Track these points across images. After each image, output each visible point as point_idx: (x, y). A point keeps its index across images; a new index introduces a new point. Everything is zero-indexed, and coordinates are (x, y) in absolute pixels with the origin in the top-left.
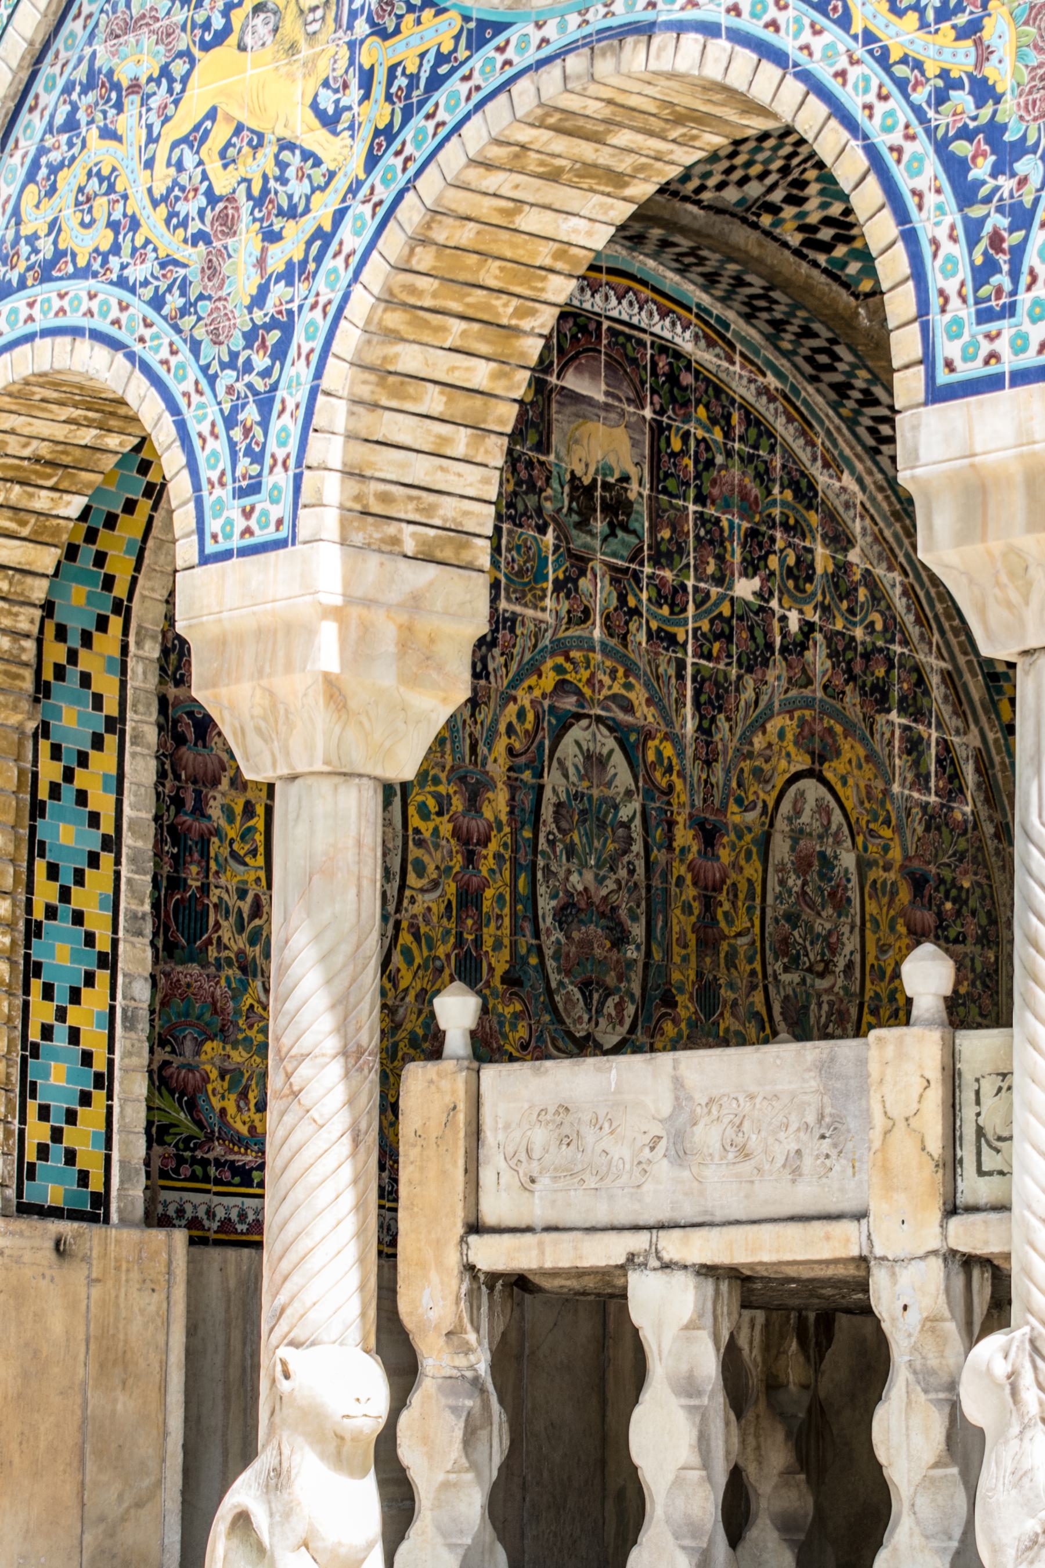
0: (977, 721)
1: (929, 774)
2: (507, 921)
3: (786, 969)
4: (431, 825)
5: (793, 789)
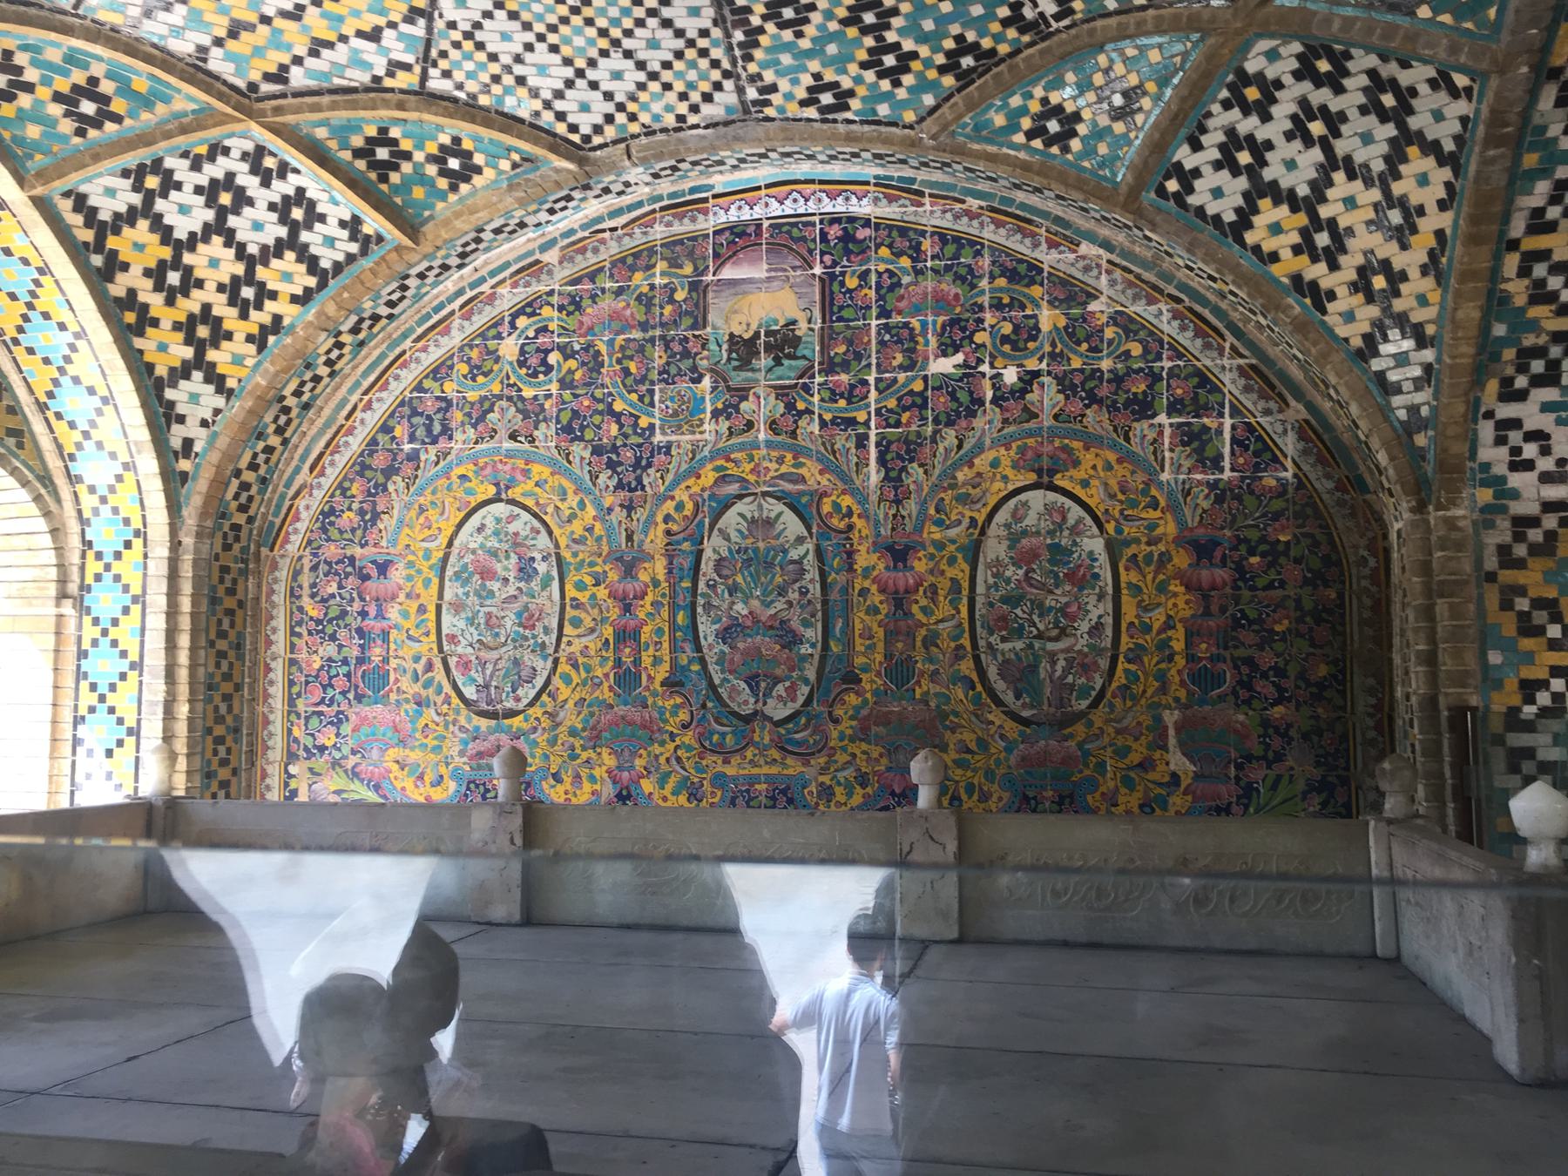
1: (1220, 457)
2: (666, 645)
3: (1004, 639)
4: (587, 594)
5: (1012, 503)
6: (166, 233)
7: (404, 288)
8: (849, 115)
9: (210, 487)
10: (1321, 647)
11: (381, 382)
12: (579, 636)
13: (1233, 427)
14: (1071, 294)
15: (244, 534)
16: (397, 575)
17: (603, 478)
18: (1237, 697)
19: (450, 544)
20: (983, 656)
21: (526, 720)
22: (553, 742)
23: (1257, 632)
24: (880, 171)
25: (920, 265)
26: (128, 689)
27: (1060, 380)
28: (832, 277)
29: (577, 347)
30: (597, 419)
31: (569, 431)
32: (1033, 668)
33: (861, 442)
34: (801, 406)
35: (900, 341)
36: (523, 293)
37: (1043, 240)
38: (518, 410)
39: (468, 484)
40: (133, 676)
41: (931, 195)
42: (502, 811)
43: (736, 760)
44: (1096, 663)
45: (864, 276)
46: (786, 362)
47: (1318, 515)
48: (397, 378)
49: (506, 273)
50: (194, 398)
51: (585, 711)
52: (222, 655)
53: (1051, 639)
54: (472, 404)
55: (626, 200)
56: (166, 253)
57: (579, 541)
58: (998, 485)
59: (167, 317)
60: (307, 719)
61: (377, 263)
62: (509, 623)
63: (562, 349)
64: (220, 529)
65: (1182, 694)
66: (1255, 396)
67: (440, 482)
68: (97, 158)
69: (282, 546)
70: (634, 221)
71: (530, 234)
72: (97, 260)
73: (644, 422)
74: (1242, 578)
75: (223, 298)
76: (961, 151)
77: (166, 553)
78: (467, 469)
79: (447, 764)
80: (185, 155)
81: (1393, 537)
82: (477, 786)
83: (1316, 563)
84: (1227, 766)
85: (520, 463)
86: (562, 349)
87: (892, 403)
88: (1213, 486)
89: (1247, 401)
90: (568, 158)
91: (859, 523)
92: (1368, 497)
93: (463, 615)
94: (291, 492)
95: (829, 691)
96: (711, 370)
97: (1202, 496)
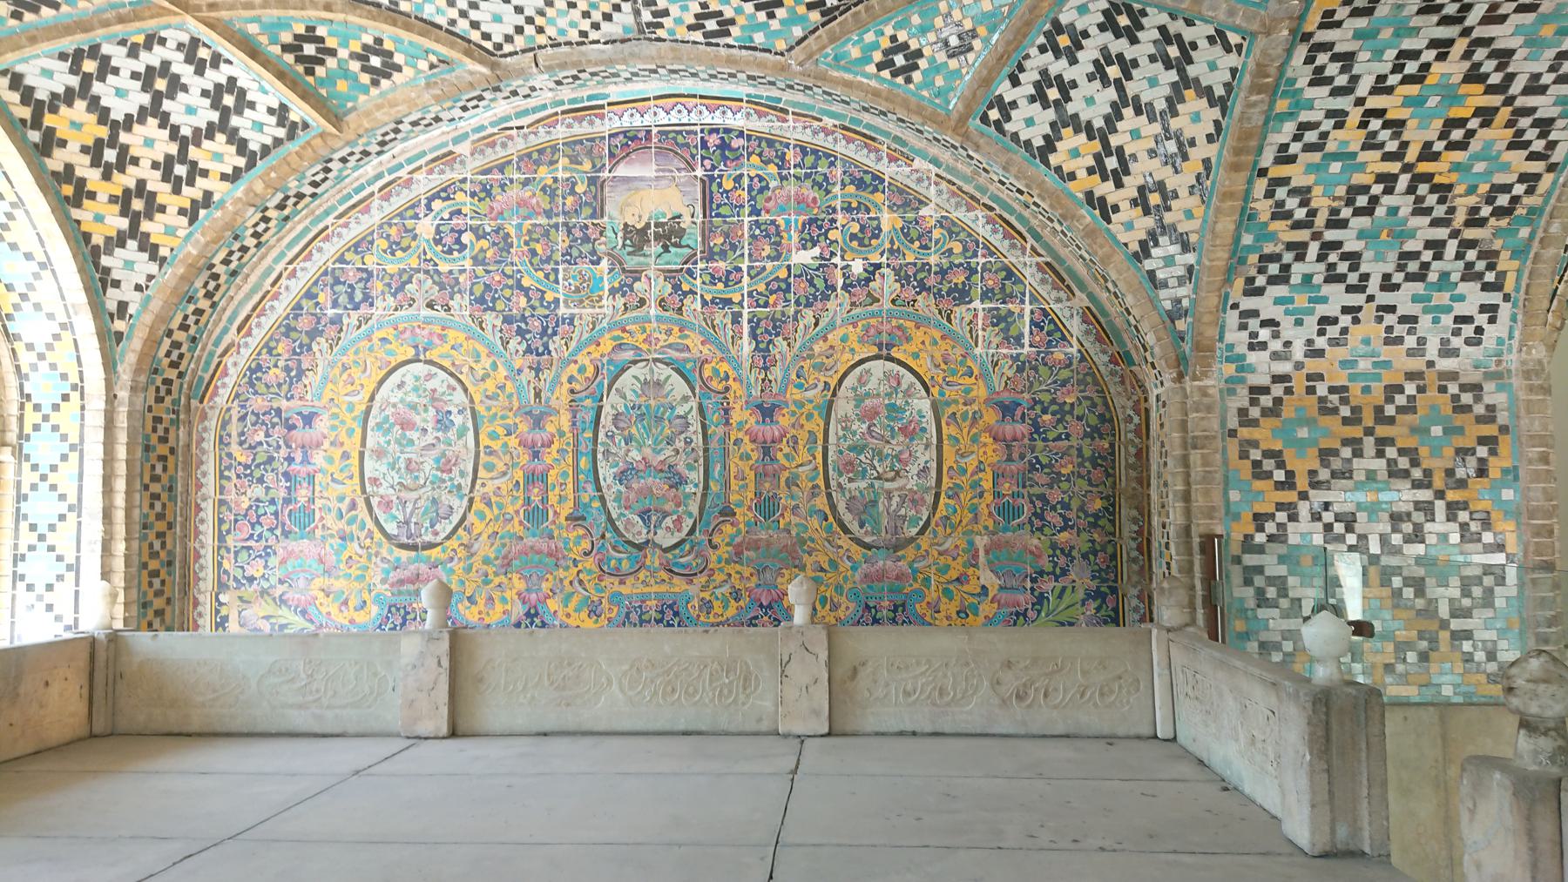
1: (1020, 336)
2: (570, 486)
3: (851, 480)
4: (500, 443)
5: (858, 370)
6: (103, 115)
7: (328, 170)
8: (729, 40)
9: (144, 345)
10: (1097, 486)
11: (305, 253)
12: (492, 479)
13: (1032, 312)
14: (908, 201)
15: (175, 388)
16: (322, 425)
17: (513, 344)
18: (1032, 526)
19: (372, 399)
20: (834, 494)
21: (444, 551)
22: (468, 570)
23: (1048, 474)
24: (752, 91)
25: (785, 172)
26: (67, 529)
27: (897, 272)
28: (712, 178)
29: (488, 229)
30: (507, 293)
31: (483, 301)
32: (874, 503)
33: (736, 318)
34: (685, 287)
35: (768, 236)
36: (437, 180)
37: (884, 155)
38: (434, 282)
39: (388, 346)
40: (72, 517)
41: (793, 113)
42: (430, 638)
43: (630, 580)
44: (922, 499)
45: (738, 179)
46: (672, 249)
47: (1096, 383)
48: (320, 250)
49: (422, 161)
50: (129, 265)
51: (498, 542)
52: (156, 497)
53: (887, 480)
54: (392, 276)
55: (531, 102)
56: (104, 132)
58: (847, 356)
59: (104, 190)
60: (236, 553)
61: (303, 148)
62: (427, 467)
63: (474, 230)
64: (153, 383)
65: (990, 523)
66: (1049, 287)
67: (363, 344)
68: (33, 40)
69: (211, 399)
70: (538, 121)
71: (444, 127)
72: (35, 136)
73: (549, 297)
74: (1037, 432)
75: (158, 174)
76: (823, 77)
77: (102, 405)
78: (388, 332)
79: (370, 591)
80: (123, 42)
81: (1152, 400)
82: (398, 610)
83: (1093, 420)
84: (1024, 580)
85: (437, 329)
86: (474, 230)
87: (762, 288)
88: (1016, 358)
89: (1044, 291)
90: (481, 62)
91: (734, 386)
92: (1133, 368)
93: (385, 461)
94: (220, 350)
95: (709, 523)
96: (609, 254)
97: (1007, 366)
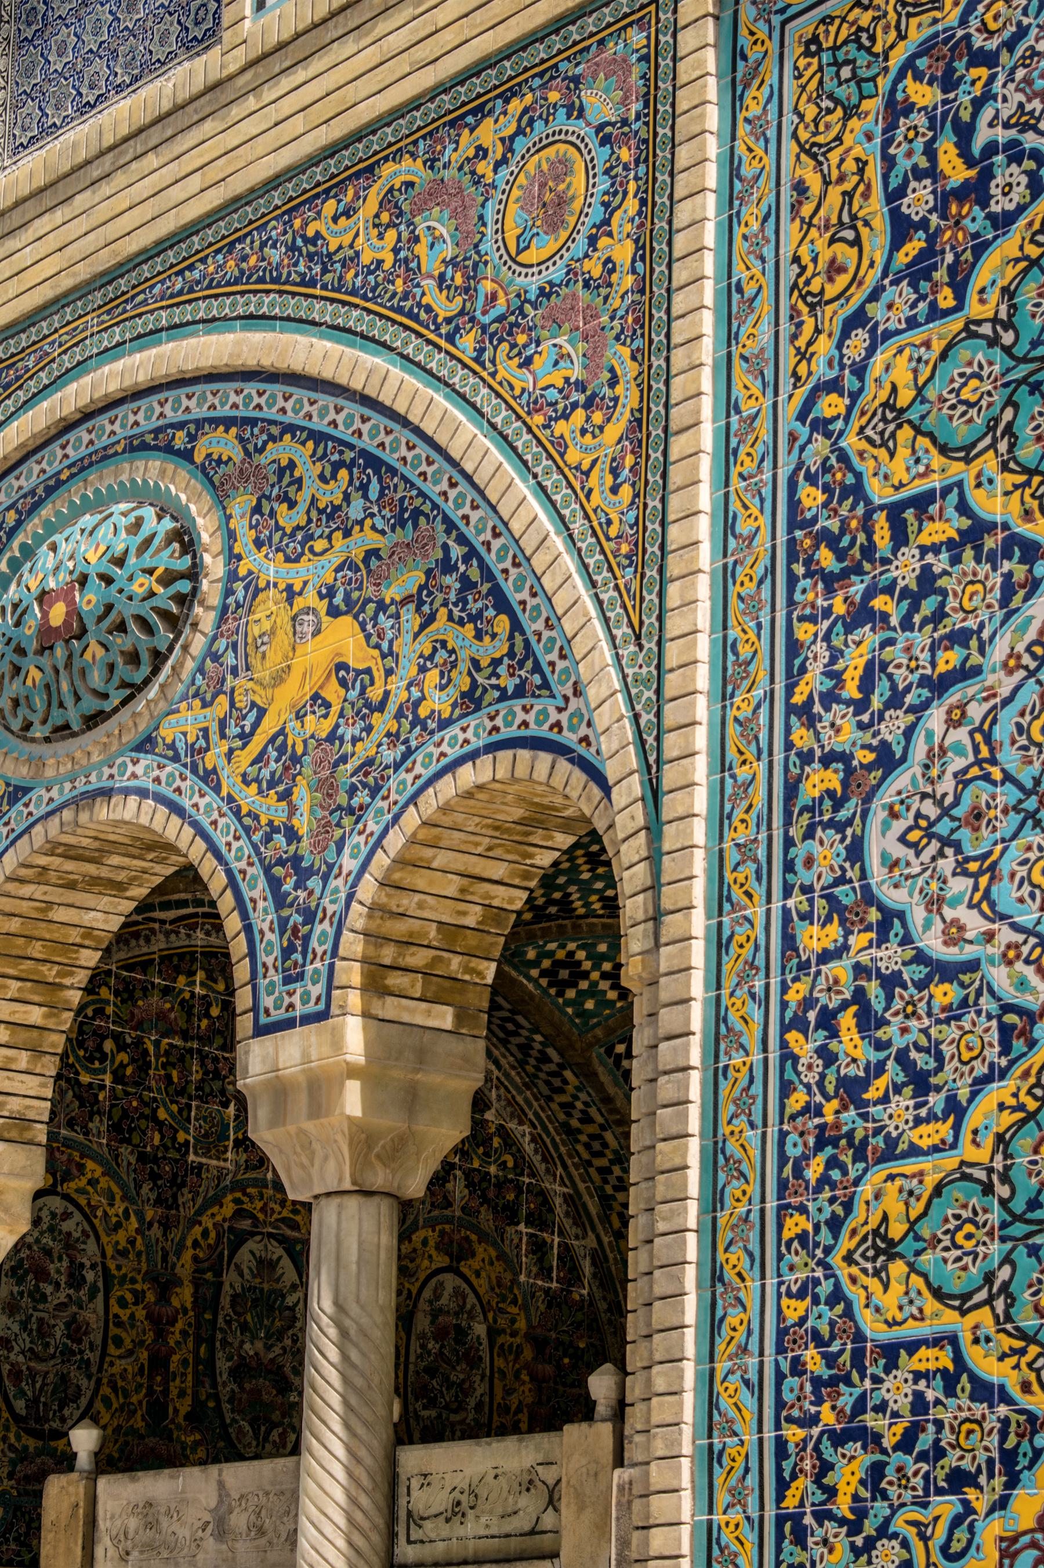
0: (594, 1229)
3: (425, 1408)
17: (145, 1189)
29: (129, 1040)
30: (143, 1123)
31: (120, 1131)
57: (123, 1253)
63: (117, 1037)
73: (181, 1137)
86: (117, 1037)
